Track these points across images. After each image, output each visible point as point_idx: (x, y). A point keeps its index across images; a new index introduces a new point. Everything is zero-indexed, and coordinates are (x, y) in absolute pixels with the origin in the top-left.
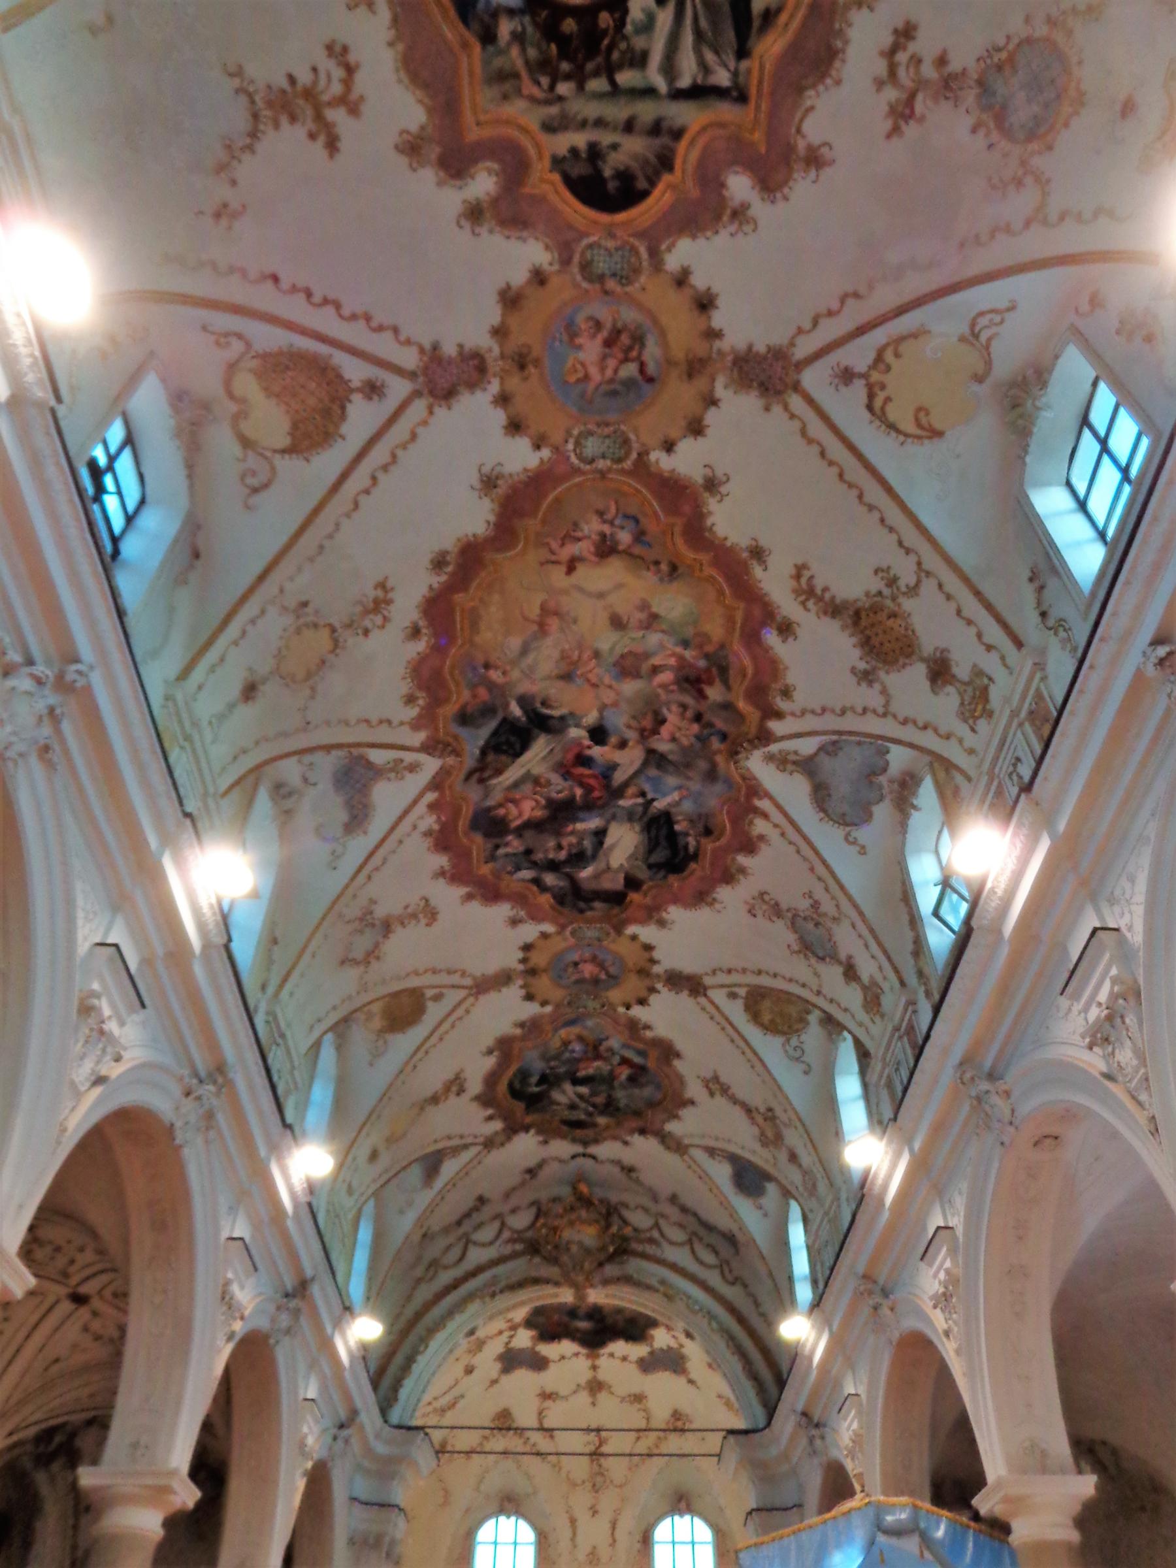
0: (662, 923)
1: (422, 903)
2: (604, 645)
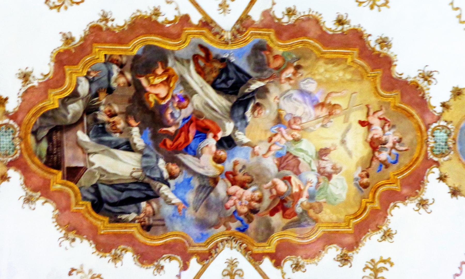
2: (303, 145)
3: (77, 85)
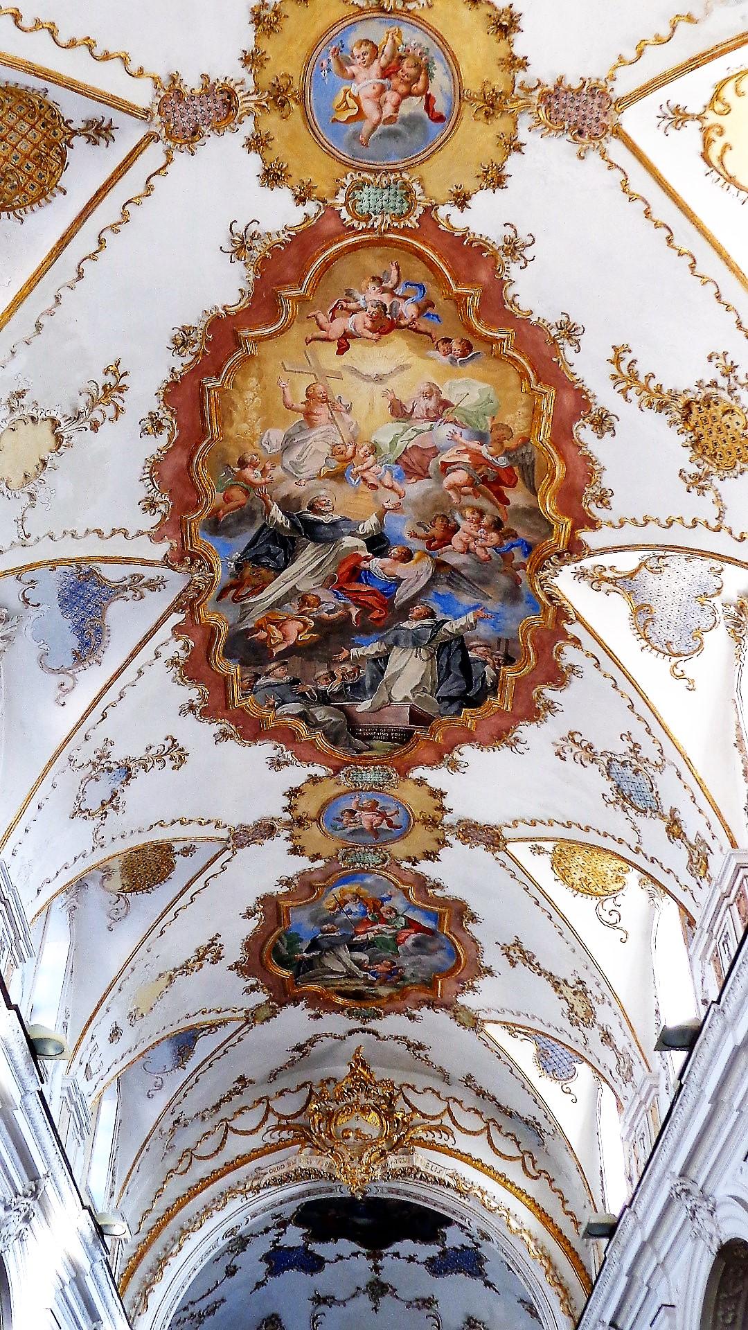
0: (454, 766)
1: (169, 743)
2: (384, 440)
3: (288, 715)
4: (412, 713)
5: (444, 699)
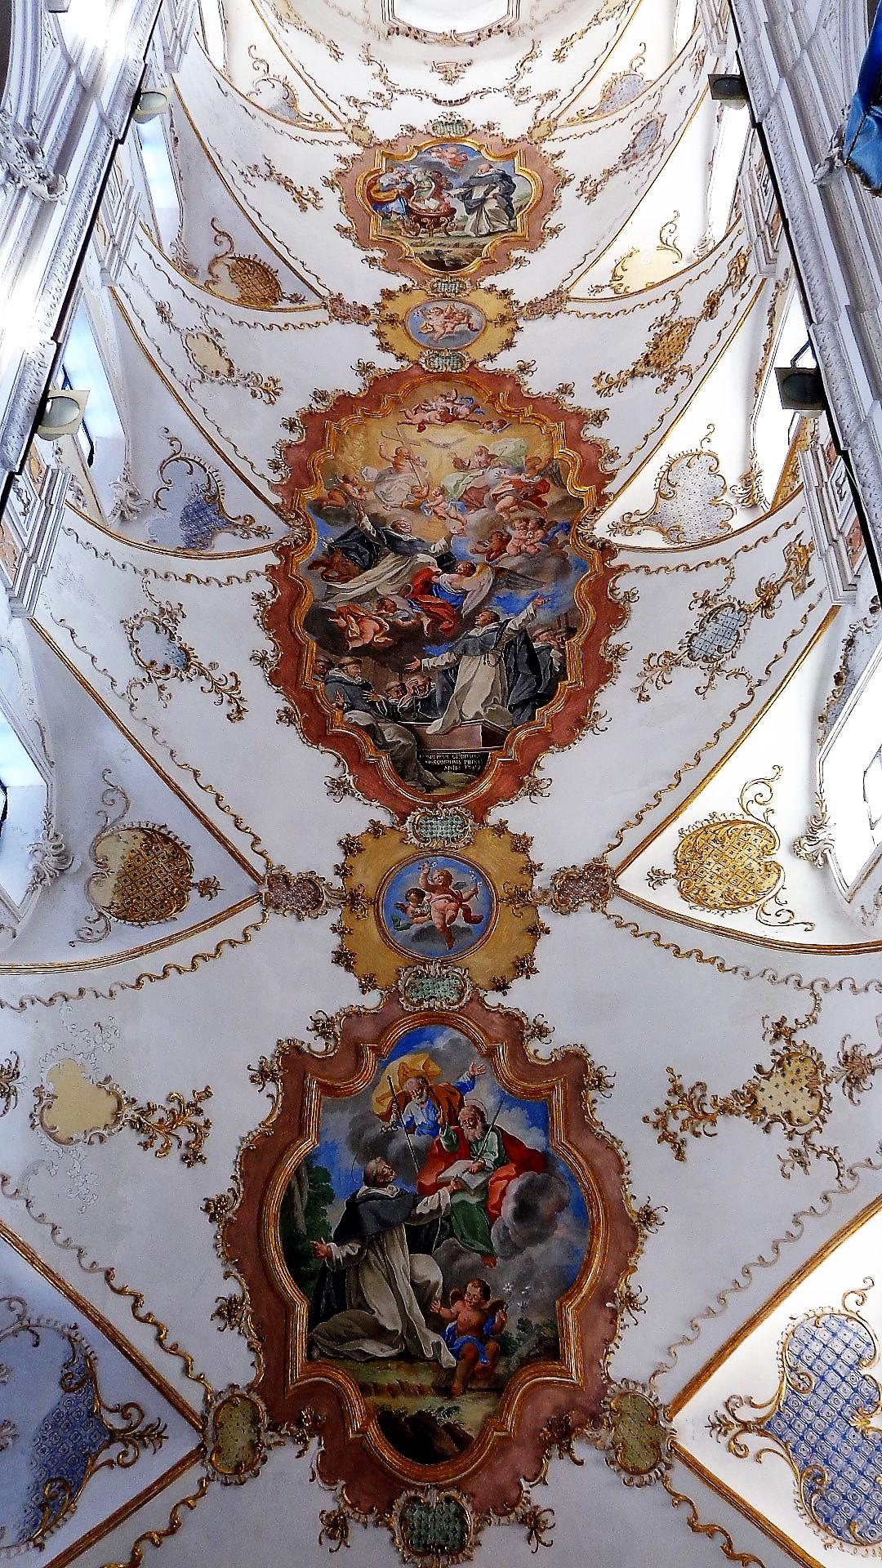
1: (232, 682)
2: (450, 485)
4: (485, 732)
5: (516, 706)
